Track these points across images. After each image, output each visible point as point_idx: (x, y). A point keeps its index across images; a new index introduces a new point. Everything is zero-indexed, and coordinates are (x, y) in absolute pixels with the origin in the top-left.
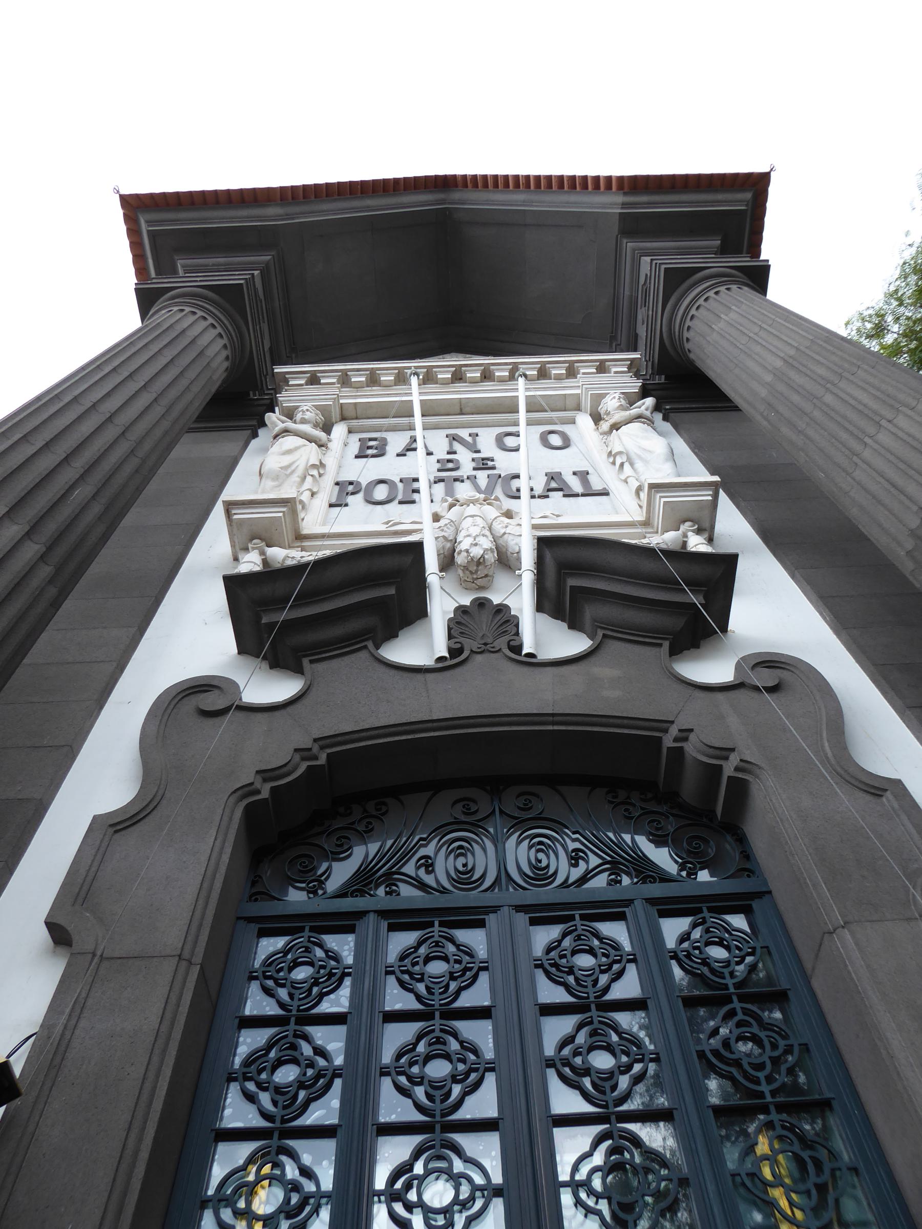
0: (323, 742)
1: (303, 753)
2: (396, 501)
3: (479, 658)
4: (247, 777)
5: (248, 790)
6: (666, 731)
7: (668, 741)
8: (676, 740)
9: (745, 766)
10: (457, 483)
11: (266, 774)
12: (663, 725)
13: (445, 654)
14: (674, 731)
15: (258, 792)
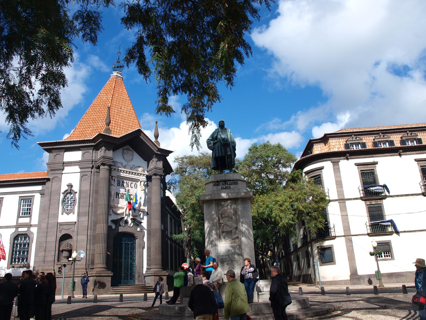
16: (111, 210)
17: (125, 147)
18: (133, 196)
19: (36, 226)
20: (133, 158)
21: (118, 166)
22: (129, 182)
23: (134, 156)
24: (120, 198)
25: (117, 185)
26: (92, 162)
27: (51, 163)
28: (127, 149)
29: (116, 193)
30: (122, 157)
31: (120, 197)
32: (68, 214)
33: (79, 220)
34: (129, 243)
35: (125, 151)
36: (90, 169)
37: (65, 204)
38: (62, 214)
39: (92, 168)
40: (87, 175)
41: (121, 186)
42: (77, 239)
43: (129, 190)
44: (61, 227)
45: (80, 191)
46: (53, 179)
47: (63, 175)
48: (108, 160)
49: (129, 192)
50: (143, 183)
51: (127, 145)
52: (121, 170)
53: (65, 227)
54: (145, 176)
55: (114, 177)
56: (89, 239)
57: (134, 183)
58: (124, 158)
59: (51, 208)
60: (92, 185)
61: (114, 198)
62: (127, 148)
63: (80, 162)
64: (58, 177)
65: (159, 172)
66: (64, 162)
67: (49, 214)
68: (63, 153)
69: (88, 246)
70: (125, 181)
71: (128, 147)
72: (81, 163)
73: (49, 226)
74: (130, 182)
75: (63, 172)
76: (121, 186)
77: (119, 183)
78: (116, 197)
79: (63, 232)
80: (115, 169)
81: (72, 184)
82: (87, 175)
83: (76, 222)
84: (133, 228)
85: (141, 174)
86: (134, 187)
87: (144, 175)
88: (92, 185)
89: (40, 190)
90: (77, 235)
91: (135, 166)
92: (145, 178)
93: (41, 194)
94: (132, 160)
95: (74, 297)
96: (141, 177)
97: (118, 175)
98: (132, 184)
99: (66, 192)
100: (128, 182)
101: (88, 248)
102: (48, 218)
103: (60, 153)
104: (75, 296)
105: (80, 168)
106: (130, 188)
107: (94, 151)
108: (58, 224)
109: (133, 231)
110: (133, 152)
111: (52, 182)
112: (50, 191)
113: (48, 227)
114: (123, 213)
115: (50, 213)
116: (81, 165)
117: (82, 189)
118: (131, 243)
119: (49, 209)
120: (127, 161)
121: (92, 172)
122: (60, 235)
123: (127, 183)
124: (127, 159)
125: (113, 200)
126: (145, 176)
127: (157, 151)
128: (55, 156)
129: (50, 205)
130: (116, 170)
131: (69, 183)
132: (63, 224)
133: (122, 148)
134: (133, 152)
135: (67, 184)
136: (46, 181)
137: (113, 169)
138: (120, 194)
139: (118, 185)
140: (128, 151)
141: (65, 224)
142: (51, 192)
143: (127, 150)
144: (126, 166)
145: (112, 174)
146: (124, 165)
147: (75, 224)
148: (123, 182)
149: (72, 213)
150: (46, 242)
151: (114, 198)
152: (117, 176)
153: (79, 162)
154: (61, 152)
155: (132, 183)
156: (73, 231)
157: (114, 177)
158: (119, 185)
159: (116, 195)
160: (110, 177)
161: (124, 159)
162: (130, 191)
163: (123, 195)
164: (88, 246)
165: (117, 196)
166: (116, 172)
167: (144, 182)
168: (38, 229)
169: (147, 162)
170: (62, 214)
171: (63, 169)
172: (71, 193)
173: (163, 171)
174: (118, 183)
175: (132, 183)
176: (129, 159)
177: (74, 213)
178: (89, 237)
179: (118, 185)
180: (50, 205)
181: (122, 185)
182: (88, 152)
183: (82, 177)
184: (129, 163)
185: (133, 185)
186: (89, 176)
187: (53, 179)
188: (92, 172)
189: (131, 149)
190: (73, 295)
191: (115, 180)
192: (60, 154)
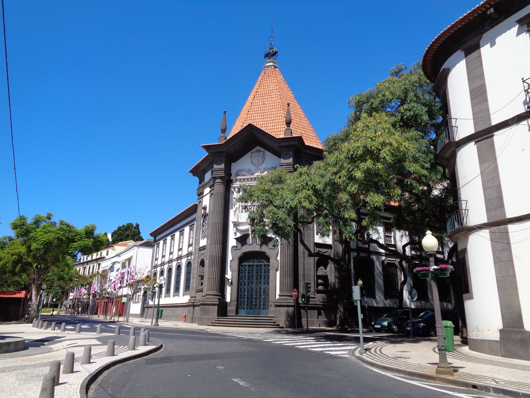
4: (238, 257)
17: (254, 150)
28: (259, 151)
32: (204, 239)
34: (261, 264)
38: (202, 239)
51: (257, 146)
58: (252, 163)
71: (258, 148)
83: (205, 246)
95: (158, 326)
104: (159, 324)
118: (264, 264)
133: (250, 152)
134: (264, 152)
163: (250, 208)
166: (239, 183)
170: (202, 239)
173: (292, 166)
187: (199, 204)
189: (262, 149)
190: (157, 323)
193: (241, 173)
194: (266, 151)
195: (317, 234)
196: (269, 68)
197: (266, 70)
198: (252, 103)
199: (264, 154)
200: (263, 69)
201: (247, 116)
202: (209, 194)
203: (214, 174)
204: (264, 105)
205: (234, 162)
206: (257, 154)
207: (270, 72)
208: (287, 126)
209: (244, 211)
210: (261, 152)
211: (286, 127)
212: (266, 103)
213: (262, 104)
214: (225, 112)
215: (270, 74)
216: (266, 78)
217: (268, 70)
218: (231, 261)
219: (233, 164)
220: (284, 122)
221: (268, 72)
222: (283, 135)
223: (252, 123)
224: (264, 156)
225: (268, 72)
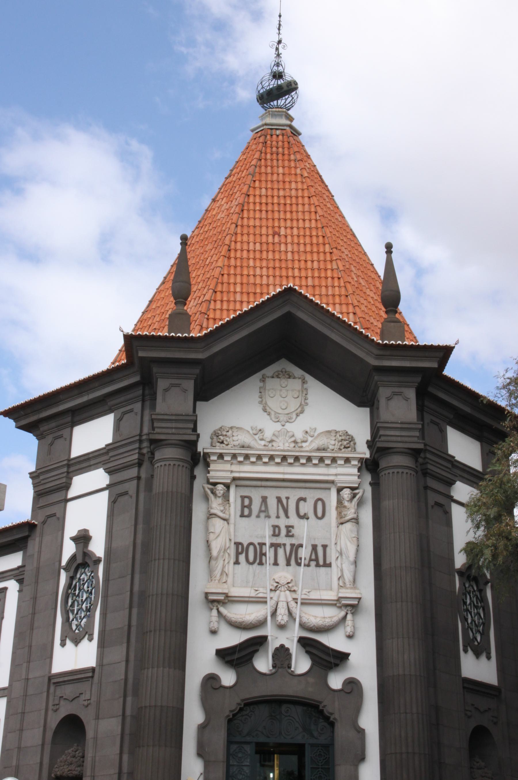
0: (242, 700)
1: (239, 704)
2: (256, 564)
3: (280, 670)
4: (227, 713)
5: (228, 716)
6: (321, 703)
7: (321, 708)
8: (323, 707)
9: (335, 719)
10: (279, 548)
11: (231, 711)
12: (321, 702)
13: (271, 668)
14: (322, 705)
15: (229, 716)
16: (215, 612)
17: (269, 371)
18: (310, 548)
19: (6, 691)
20: (307, 404)
21: (236, 443)
22: (287, 498)
23: (308, 396)
24: (252, 564)
25: (239, 513)
26: (141, 441)
27: (39, 471)
29: (235, 543)
30: (260, 408)
31: (251, 558)
32: (77, 642)
33: (105, 661)
35: (271, 383)
36: (133, 472)
37: (73, 605)
38: (63, 644)
39: (140, 464)
40: (126, 493)
41: (258, 516)
42: (96, 731)
43: (289, 528)
44: (60, 691)
45: (109, 550)
46: (44, 523)
47: (70, 505)
48: (174, 425)
49: (292, 536)
50: (346, 493)
52: (247, 457)
53: (68, 691)
54: (354, 466)
55: (220, 487)
56: (127, 731)
57: (311, 495)
58: (265, 410)
59: (36, 624)
60: (140, 527)
61: (224, 567)
62: (279, 369)
63: (107, 453)
64: (54, 515)
65: (399, 439)
66: (69, 460)
67: (30, 647)
68: (69, 429)
69: (125, 757)
70: (272, 495)
71: (284, 364)
72: (111, 454)
73: (30, 691)
74: (294, 495)
75: (70, 495)
76: (258, 516)
77: (249, 507)
78: (237, 562)
79: (63, 713)
80: (221, 456)
81: (91, 534)
82: (126, 493)
83: (93, 670)
84: (311, 680)
85: (334, 460)
86: (311, 514)
87: (347, 460)
88: (140, 527)
89: (19, 568)
90: (97, 718)
91: (316, 434)
92: (355, 471)
93: (18, 581)
94: (302, 412)
96: (340, 470)
97: (237, 475)
98: (302, 503)
99: (75, 565)
100: (283, 494)
101: (125, 769)
102: (29, 662)
103: (60, 433)
105: (110, 472)
106: (293, 520)
107: (148, 403)
108: (53, 681)
109: (310, 689)
110: (304, 382)
111: (42, 535)
112: (35, 565)
113: (25, 695)
114: (261, 624)
115: (34, 644)
116: (112, 459)
117: (114, 545)
119: (32, 629)
120: (281, 419)
121: (139, 478)
122: (54, 721)
123: (279, 500)
124: (280, 411)
125: (221, 574)
126: (354, 466)
127: (378, 357)
128: (51, 444)
129: (34, 614)
130: (227, 458)
131: (79, 531)
132: (61, 679)
133: (259, 375)
134: (304, 382)
135: (74, 534)
136: (27, 534)
137: (214, 458)
138: (251, 548)
139: (242, 515)
140: (283, 380)
141: (66, 679)
142: (38, 569)
143: (278, 377)
144: (274, 438)
145: (212, 474)
146: (268, 435)
147: (92, 677)
148: (264, 499)
149: (87, 636)
150: (19, 748)
151: (224, 567)
152: (234, 479)
153: (108, 450)
154: (59, 428)
155: (304, 499)
156: (86, 703)
157: (220, 487)
158: (249, 516)
159: (232, 551)
160: (207, 487)
161: (269, 414)
162: (293, 531)
164: (125, 757)
165: (242, 558)
166: (228, 467)
167: (353, 489)
168: (8, 703)
169: (368, 409)
170: (63, 644)
171: (67, 486)
172: (84, 565)
174: (243, 507)
175: (304, 499)
176: (286, 411)
177: (91, 639)
178: (128, 720)
179: (242, 515)
180: (34, 614)
181: (260, 511)
182: (131, 411)
183: (113, 503)
184: (288, 426)
185: (306, 508)
186: (131, 497)
187: (44, 523)
188: (139, 478)
189: (298, 372)
191: (226, 497)
192: (61, 437)
193: (235, 438)
194: (308, 377)
195: (466, 651)
196: (278, 132)
197: (268, 137)
198: (237, 226)
199: (302, 386)
200: (252, 131)
201: (226, 263)
202: (106, 493)
203: (157, 430)
204: (276, 237)
205: (206, 398)
206: (284, 382)
207: (280, 144)
208: (386, 312)
209: (242, 558)
210: (294, 378)
211: (385, 316)
212: (283, 232)
213: (270, 232)
214: (184, 239)
215: (280, 150)
216: (272, 160)
217: (274, 137)
218: (202, 728)
219: (198, 403)
220: (170, 289)
221: (274, 143)
222: (166, 328)
223: (297, 288)
224: (305, 392)
225: (274, 143)
